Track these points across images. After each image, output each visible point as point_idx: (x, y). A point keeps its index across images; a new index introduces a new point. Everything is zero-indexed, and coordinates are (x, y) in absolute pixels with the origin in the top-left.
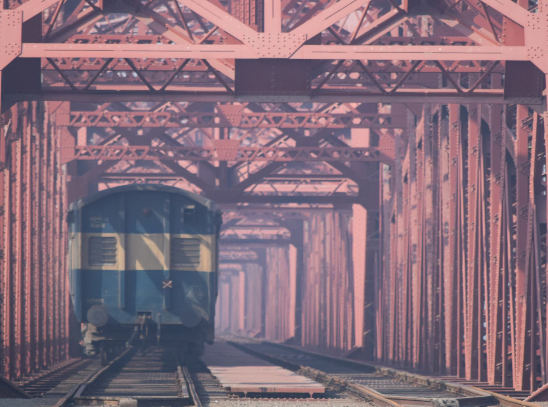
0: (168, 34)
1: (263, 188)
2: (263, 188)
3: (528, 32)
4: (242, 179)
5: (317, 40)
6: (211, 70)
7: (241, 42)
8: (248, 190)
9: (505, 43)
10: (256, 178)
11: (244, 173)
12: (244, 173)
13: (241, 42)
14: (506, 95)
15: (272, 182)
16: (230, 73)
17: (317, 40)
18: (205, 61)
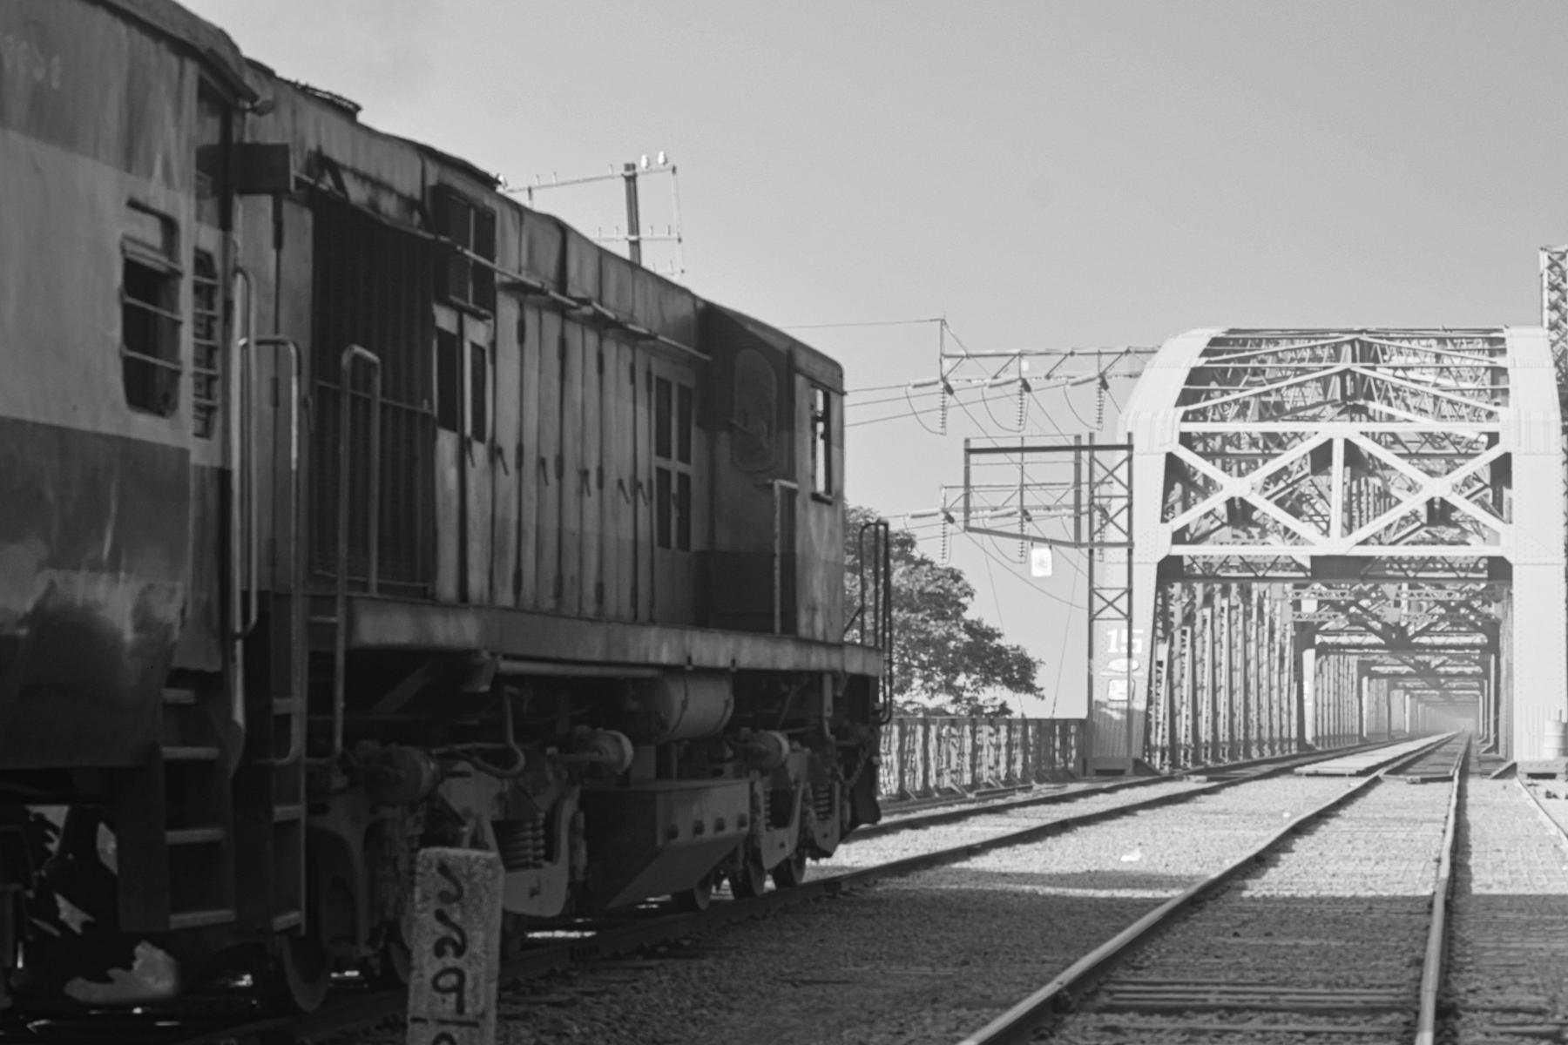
0: (1268, 539)
1: (1425, 640)
2: (1425, 640)
3: (1503, 538)
4: (1410, 634)
5: (1365, 542)
6: (1294, 561)
7: (1311, 544)
8: (1415, 641)
9: (1490, 544)
10: (1418, 634)
11: (1411, 630)
12: (1411, 630)
13: (1311, 544)
14: (1489, 579)
15: (1431, 636)
16: (1308, 564)
17: (1365, 542)
18: (1291, 557)
